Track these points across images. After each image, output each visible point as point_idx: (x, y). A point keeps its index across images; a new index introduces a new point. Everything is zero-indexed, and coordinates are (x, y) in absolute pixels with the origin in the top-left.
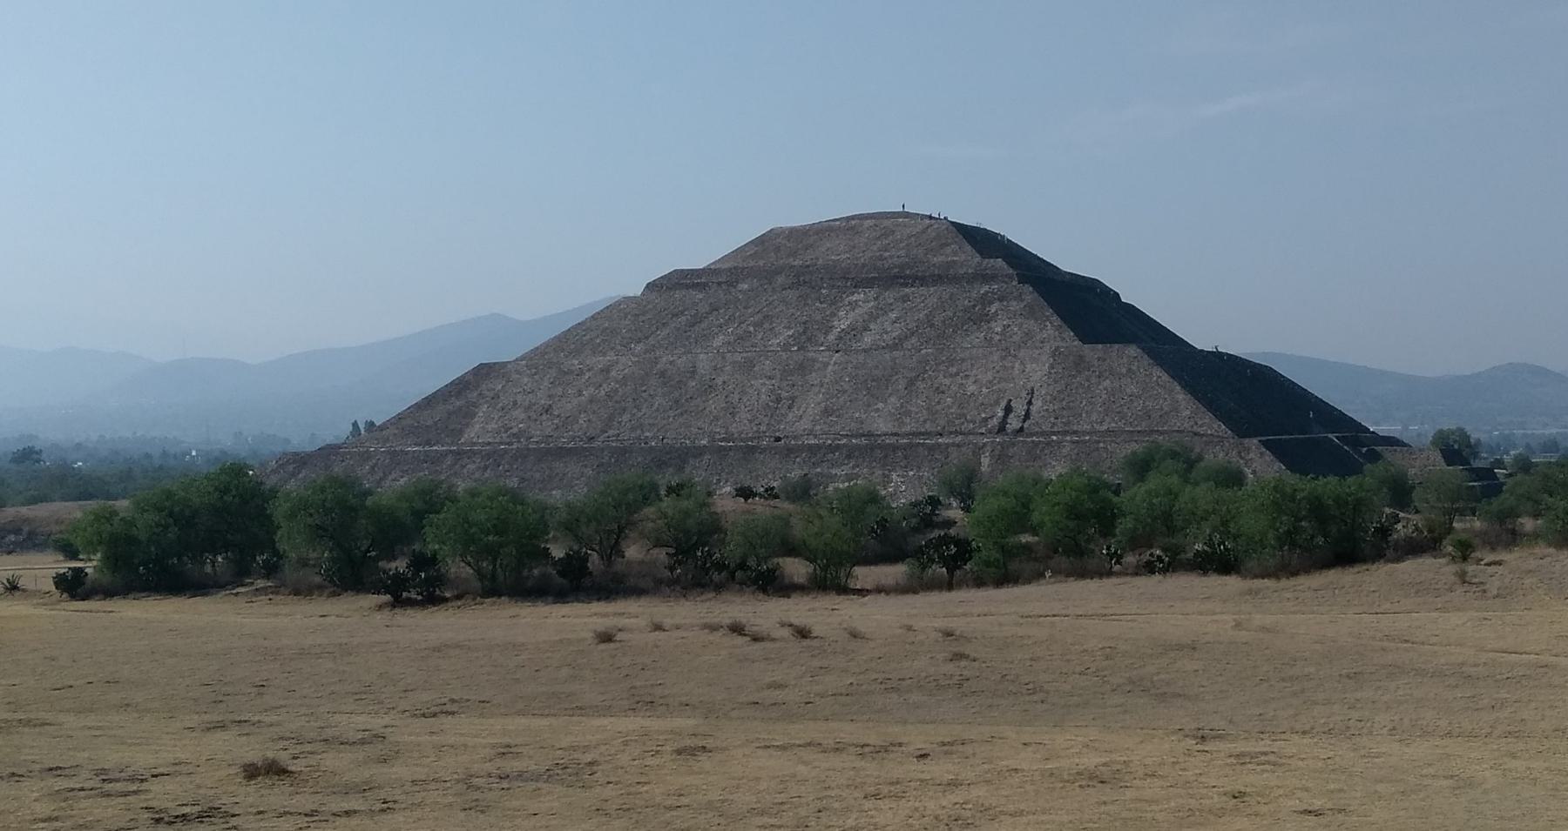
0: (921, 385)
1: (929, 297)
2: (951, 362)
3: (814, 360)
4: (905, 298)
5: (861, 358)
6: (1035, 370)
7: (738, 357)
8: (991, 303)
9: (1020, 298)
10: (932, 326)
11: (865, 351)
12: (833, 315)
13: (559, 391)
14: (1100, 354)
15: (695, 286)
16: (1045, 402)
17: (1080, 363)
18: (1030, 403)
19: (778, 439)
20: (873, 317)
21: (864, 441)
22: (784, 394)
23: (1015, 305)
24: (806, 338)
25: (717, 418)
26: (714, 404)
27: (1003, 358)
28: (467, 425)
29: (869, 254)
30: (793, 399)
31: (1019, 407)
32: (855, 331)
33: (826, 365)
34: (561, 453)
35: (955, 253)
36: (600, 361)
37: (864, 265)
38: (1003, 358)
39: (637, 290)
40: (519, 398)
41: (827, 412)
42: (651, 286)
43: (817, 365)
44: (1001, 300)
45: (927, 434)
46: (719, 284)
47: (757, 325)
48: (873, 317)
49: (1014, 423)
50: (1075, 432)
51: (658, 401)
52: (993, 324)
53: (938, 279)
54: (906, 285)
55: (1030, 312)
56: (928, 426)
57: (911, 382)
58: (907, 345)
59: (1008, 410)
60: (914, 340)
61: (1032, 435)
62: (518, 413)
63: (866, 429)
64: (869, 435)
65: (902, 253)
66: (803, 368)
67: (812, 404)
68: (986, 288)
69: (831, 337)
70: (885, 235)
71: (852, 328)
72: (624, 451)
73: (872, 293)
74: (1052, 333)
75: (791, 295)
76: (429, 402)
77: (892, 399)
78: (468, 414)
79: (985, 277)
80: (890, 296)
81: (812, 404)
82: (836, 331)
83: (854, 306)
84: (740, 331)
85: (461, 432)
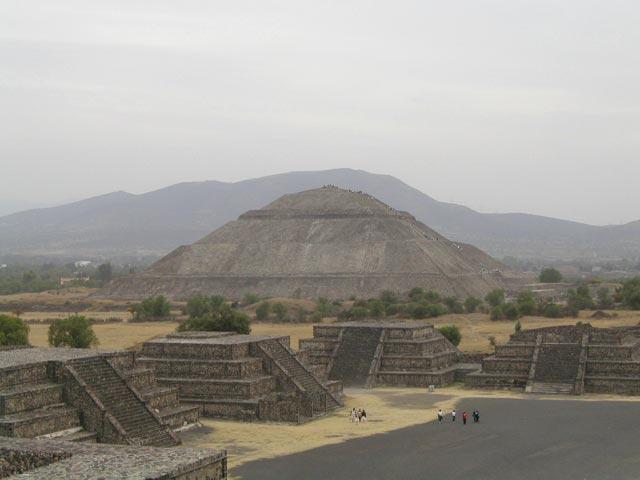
6: (380, 251)
32: (317, 234)
34: (213, 279)
42: (242, 217)
64: (321, 274)
71: (315, 234)
72: (237, 279)
73: (323, 220)
75: (293, 220)
76: (164, 259)
80: (328, 221)
83: (315, 225)
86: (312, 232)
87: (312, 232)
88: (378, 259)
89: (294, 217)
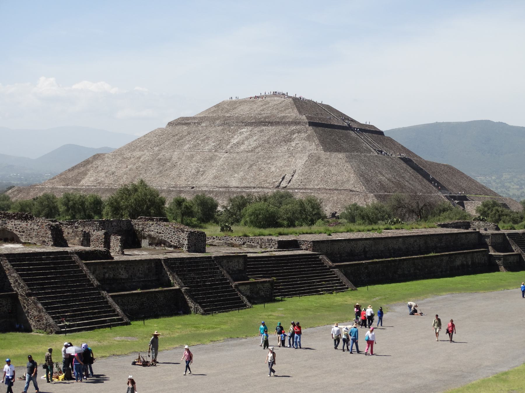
0: (254, 167)
1: (271, 130)
2: (269, 158)
3: (216, 156)
4: (262, 131)
5: (235, 155)
6: (300, 163)
7: (189, 154)
8: (294, 134)
9: (306, 132)
10: (268, 143)
11: (237, 153)
12: (232, 137)
13: (120, 166)
14: (327, 157)
15: (186, 124)
16: (299, 176)
17: (318, 159)
18: (293, 176)
19: (193, 188)
20: (247, 138)
21: (224, 190)
22: (201, 169)
23: (303, 135)
24: (218, 148)
25: (173, 179)
26: (174, 173)
27: (289, 157)
28: (83, 179)
29: (256, 112)
30: (204, 172)
31: (288, 177)
33: (220, 158)
35: (289, 113)
36: (137, 154)
37: (251, 117)
38: (289, 157)
39: (163, 125)
40: (105, 168)
41: (215, 177)
42: (170, 124)
43: (217, 158)
44: (298, 133)
45: (250, 187)
46: (195, 123)
47: (203, 140)
48: (247, 138)
49: (284, 184)
50: (305, 189)
51: (155, 170)
52: (292, 143)
53: (277, 123)
54: (265, 125)
55: (308, 138)
56: (252, 185)
57: (251, 166)
58: (257, 150)
59: (283, 178)
60: (260, 148)
61: (289, 189)
62: (103, 174)
63: (228, 184)
64: (228, 187)
65: (269, 112)
66: (211, 159)
67: (211, 173)
68: (294, 128)
69: (229, 147)
70: (265, 104)
71: (238, 143)
73: (250, 128)
74: (314, 147)
75: (221, 128)
77: (241, 173)
78: (85, 174)
79: (296, 123)
80: (256, 130)
81: (211, 173)
82: (231, 144)
84: (195, 143)
85: (80, 181)
86: (234, 141)
87: (234, 141)
88: (295, 172)
89: (223, 124)
